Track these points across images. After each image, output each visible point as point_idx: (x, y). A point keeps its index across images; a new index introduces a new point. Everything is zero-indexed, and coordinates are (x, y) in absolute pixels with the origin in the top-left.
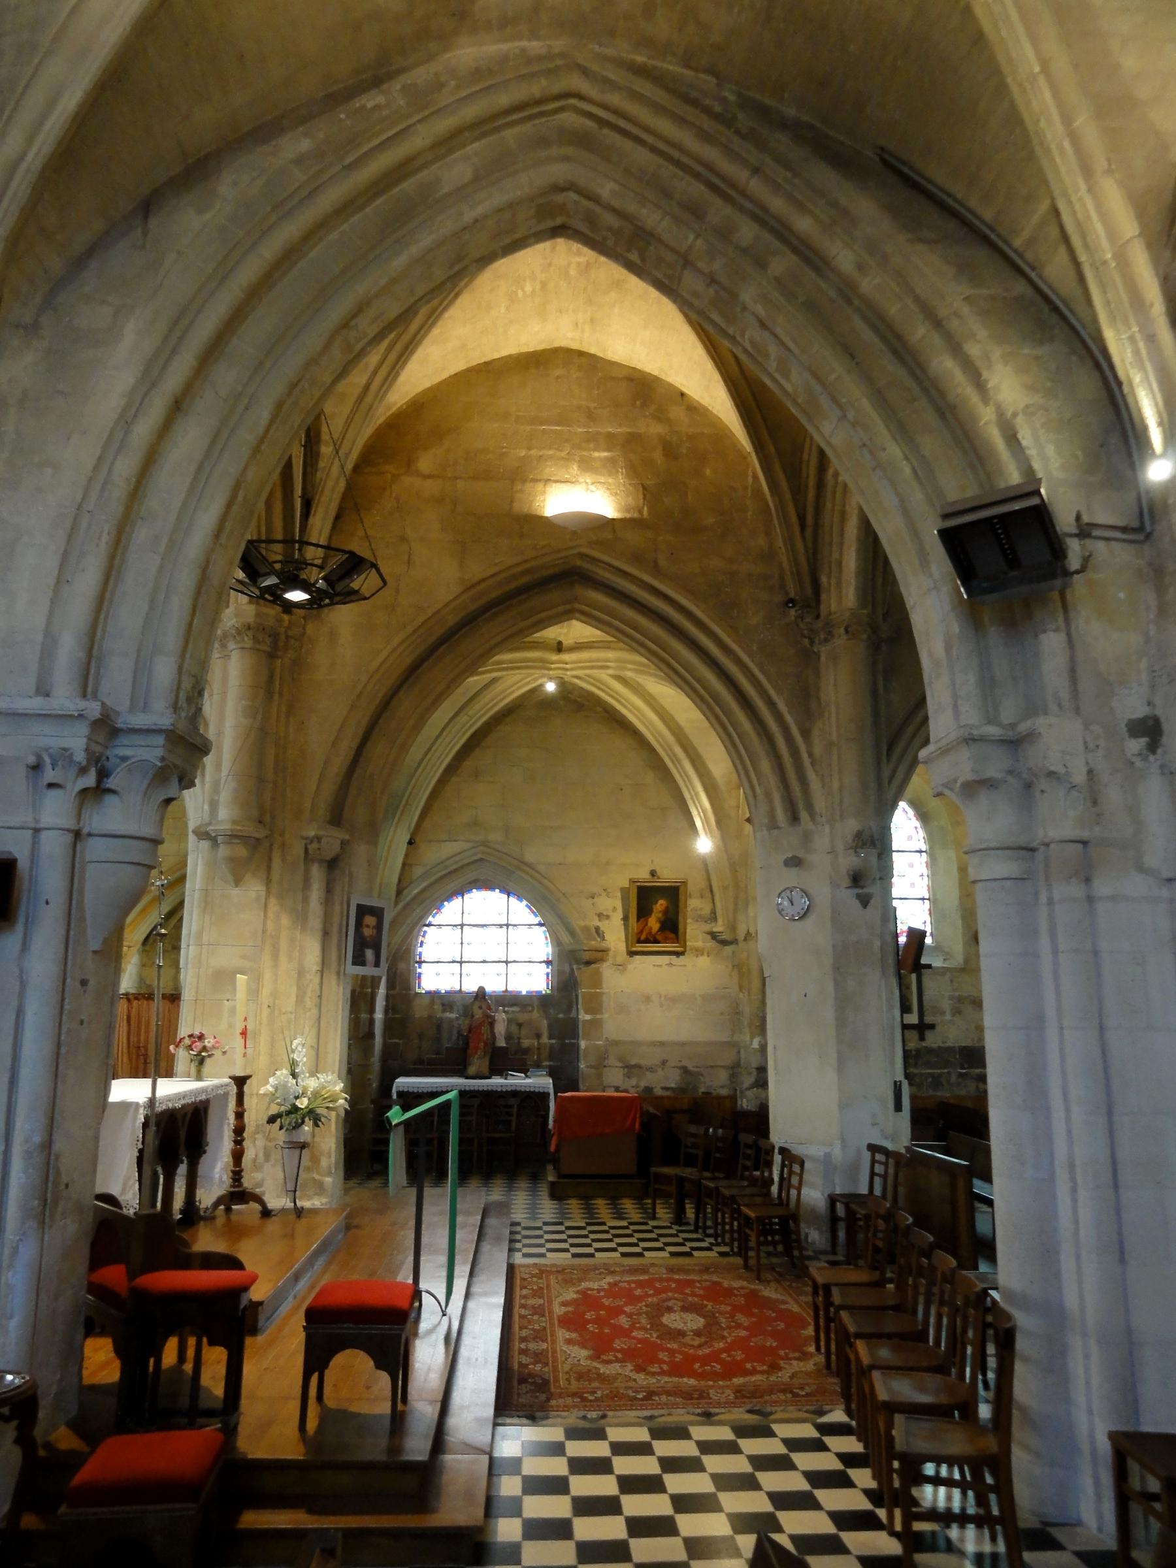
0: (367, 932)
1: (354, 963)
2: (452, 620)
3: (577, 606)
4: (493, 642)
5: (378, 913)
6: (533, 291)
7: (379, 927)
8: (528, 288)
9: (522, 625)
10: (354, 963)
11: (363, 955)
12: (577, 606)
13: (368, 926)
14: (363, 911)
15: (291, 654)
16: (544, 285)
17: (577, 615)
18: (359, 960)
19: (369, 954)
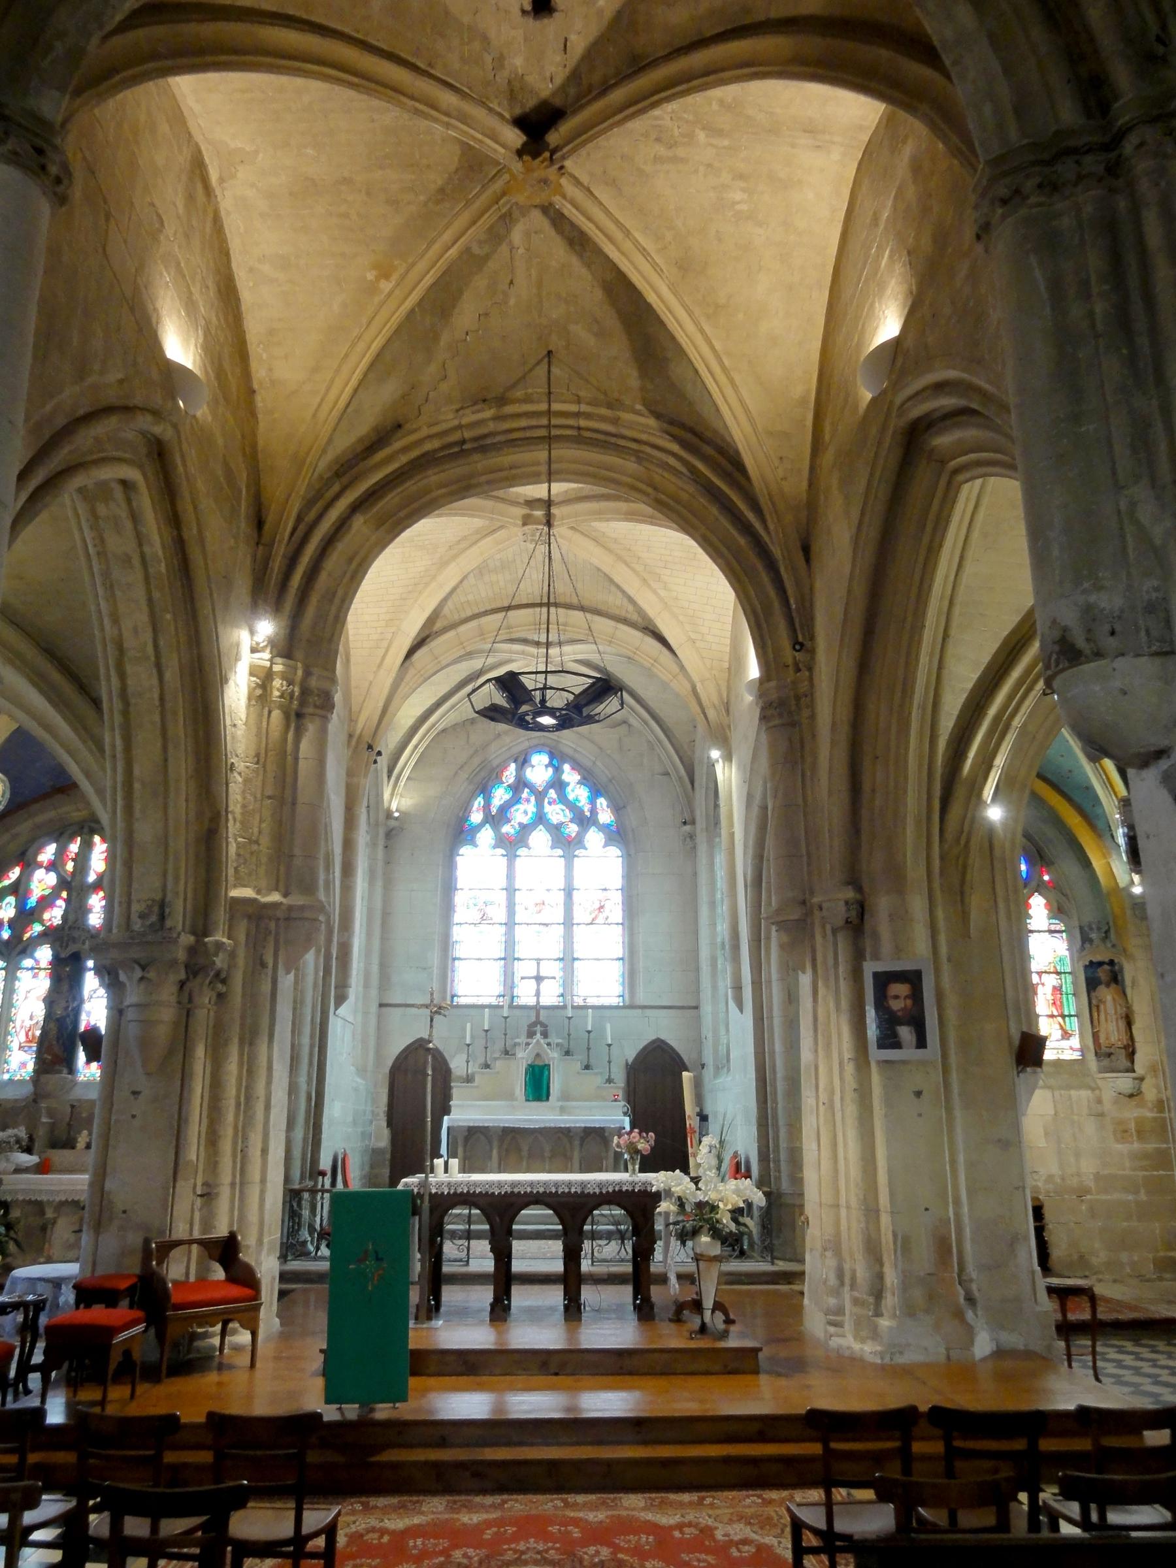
0: (896, 1005)
1: (881, 1045)
2: (860, 590)
3: (953, 464)
4: (917, 577)
5: (913, 979)
6: (743, 190)
7: (917, 995)
8: (738, 196)
9: (926, 539)
10: (881, 1045)
11: (895, 1035)
12: (953, 464)
13: (896, 997)
14: (883, 981)
15: (806, 713)
16: (741, 177)
17: (960, 477)
18: (889, 1040)
19: (905, 1033)
